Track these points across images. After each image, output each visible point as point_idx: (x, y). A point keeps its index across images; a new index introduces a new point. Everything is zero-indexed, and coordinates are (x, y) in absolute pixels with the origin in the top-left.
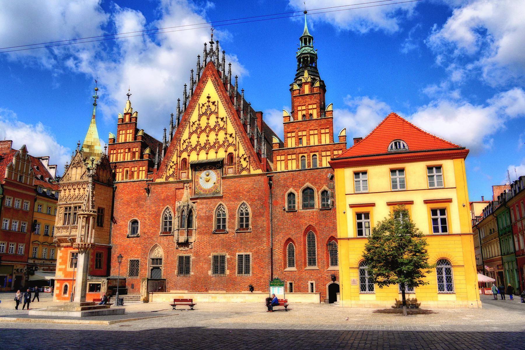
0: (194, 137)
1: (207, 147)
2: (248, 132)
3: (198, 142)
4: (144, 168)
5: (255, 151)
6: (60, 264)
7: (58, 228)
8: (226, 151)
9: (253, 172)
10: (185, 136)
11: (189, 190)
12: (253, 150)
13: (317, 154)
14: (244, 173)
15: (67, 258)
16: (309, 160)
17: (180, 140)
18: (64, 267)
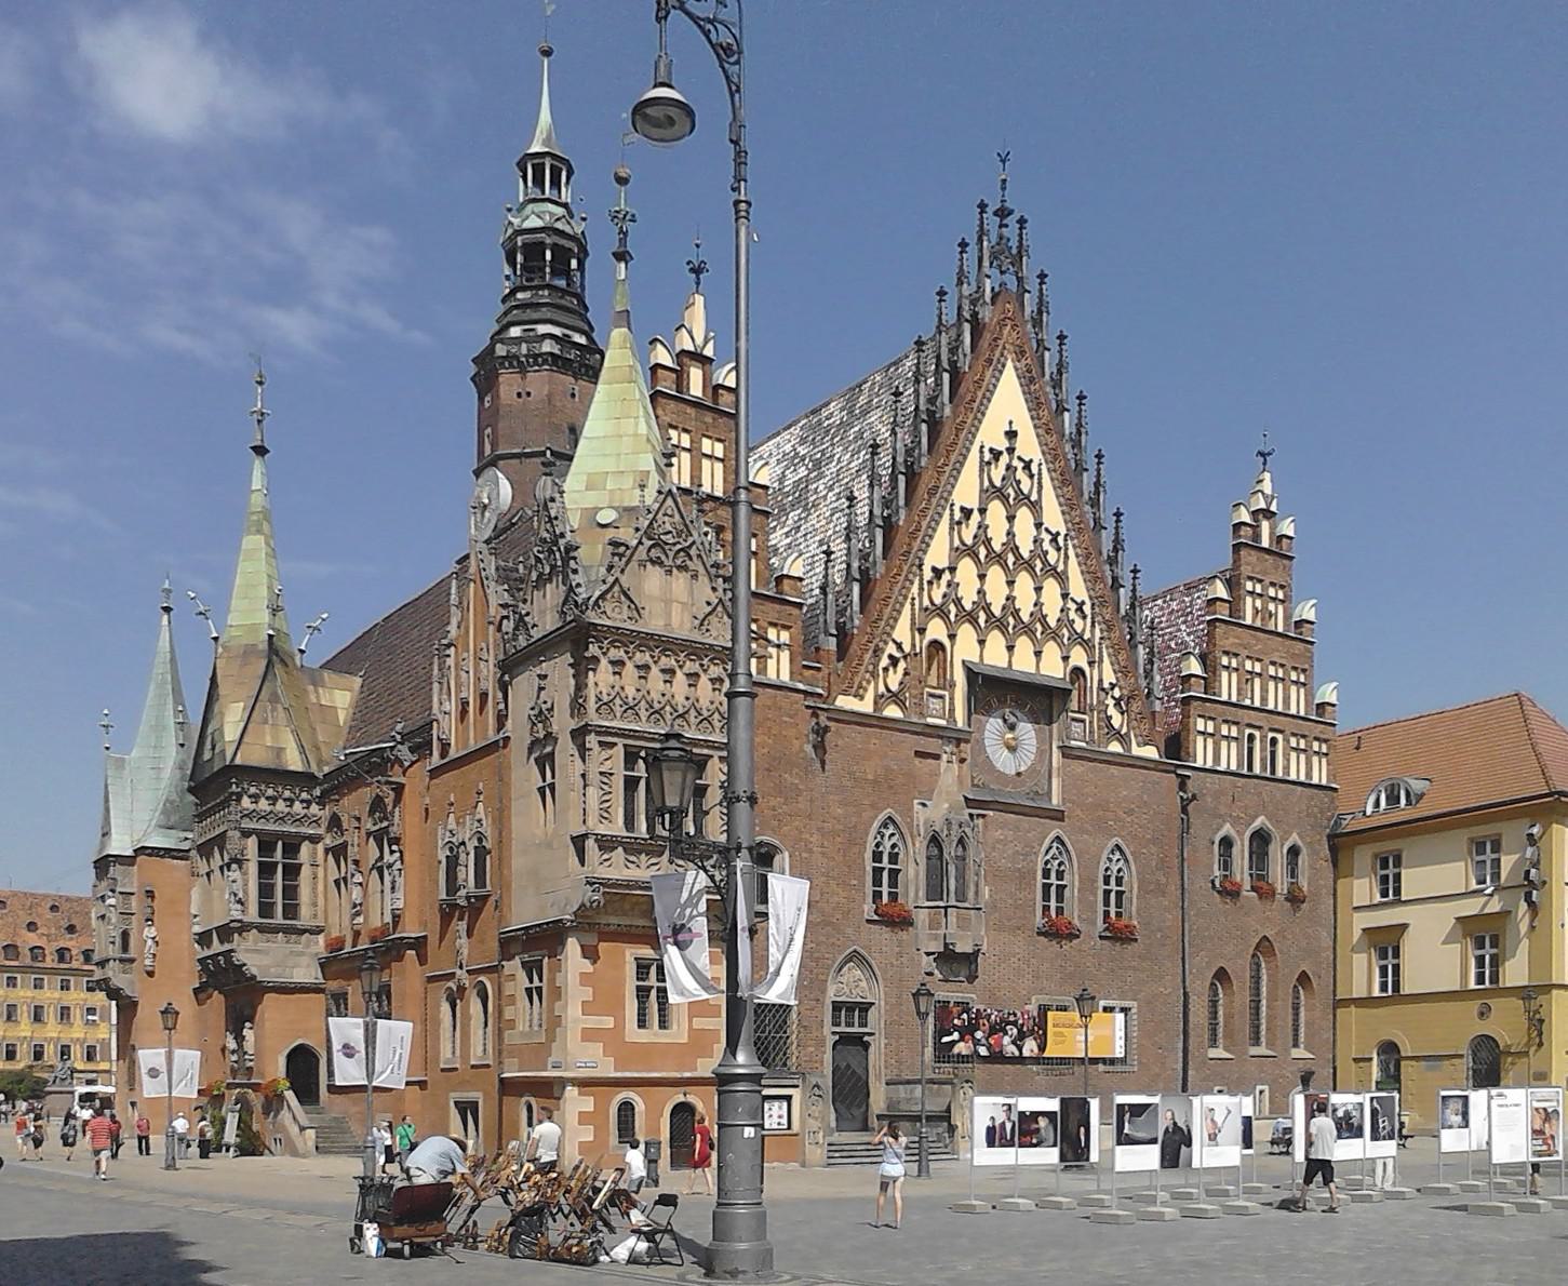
0: (967, 568)
1: (1008, 623)
2: (1123, 612)
3: (980, 592)
4: (785, 636)
5: (1144, 683)
6: (587, 1009)
7: (607, 844)
8: (1066, 659)
9: (1136, 751)
10: (937, 553)
11: (955, 766)
12: (1136, 680)
13: (1280, 737)
14: (1115, 747)
15: (621, 984)
16: (1263, 749)
17: (920, 566)
18: (609, 1022)
